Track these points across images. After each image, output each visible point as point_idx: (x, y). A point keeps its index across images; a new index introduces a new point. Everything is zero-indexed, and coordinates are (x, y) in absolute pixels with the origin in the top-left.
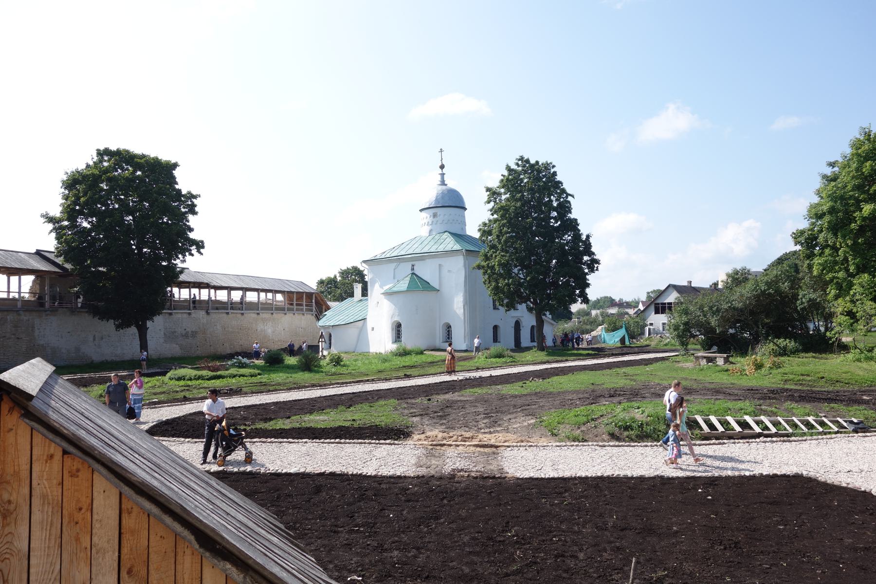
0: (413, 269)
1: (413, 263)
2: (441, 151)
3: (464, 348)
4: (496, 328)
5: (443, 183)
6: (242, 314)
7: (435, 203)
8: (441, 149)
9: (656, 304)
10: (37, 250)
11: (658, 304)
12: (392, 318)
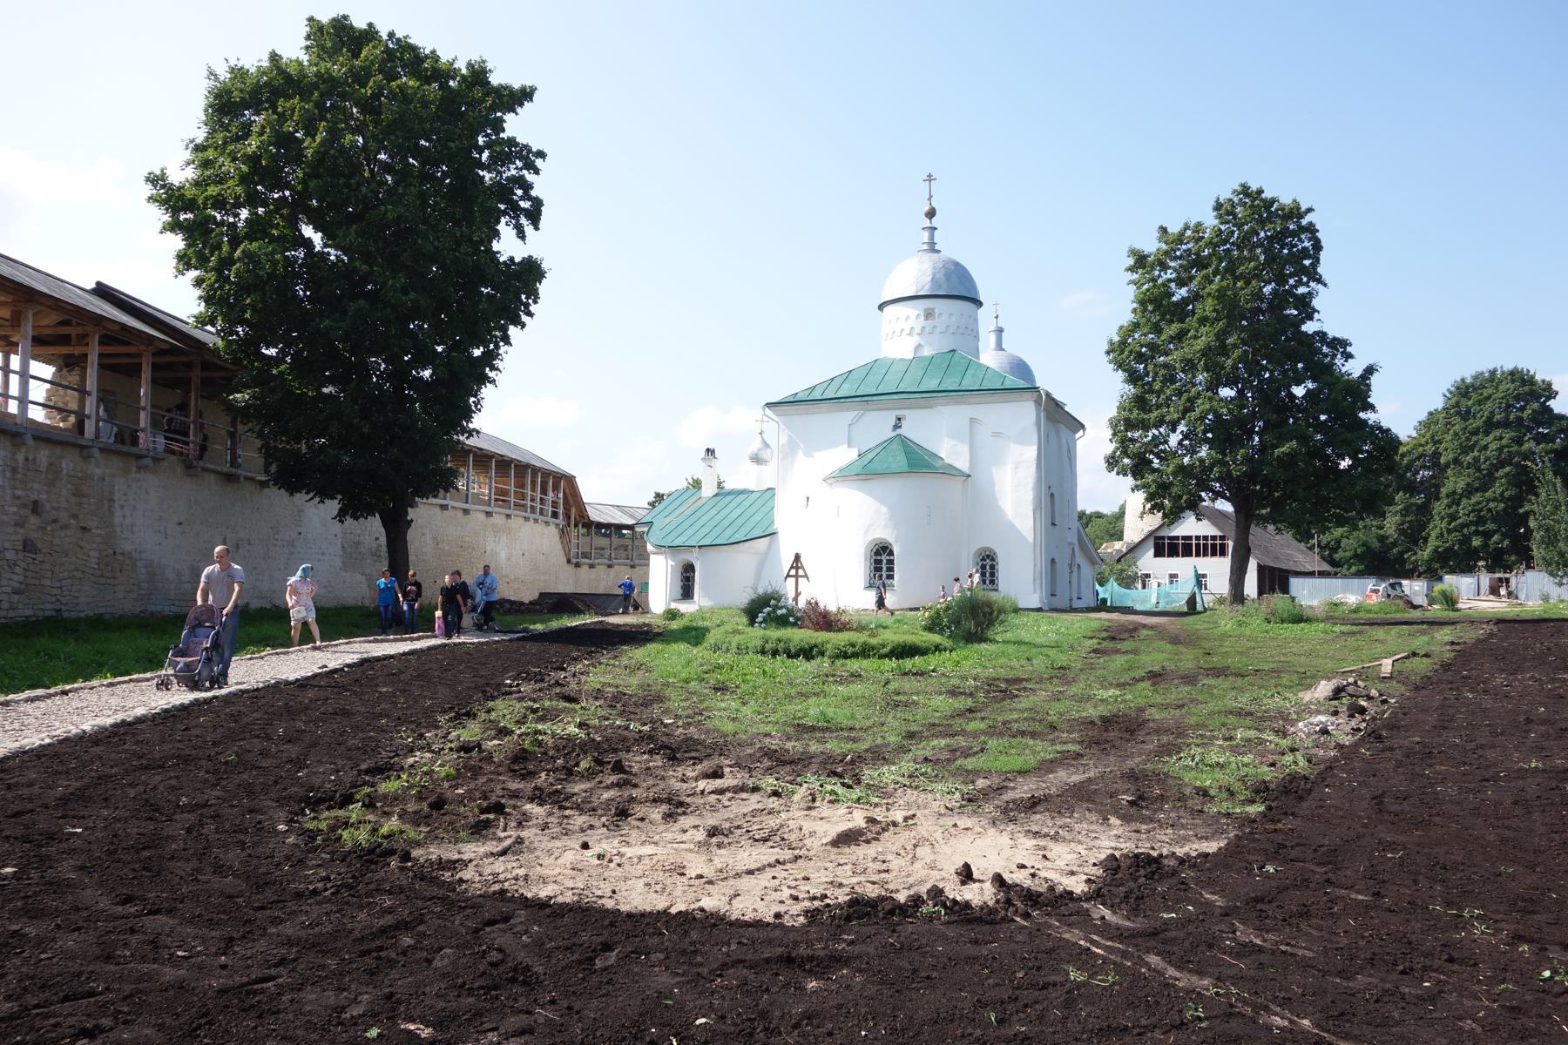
0: (897, 427)
1: (900, 413)
2: (930, 178)
3: (1036, 605)
4: (1053, 560)
5: (932, 247)
6: (466, 512)
7: (931, 288)
8: (930, 176)
9: (1156, 538)
10: (98, 284)
11: (1163, 538)
12: (867, 530)
